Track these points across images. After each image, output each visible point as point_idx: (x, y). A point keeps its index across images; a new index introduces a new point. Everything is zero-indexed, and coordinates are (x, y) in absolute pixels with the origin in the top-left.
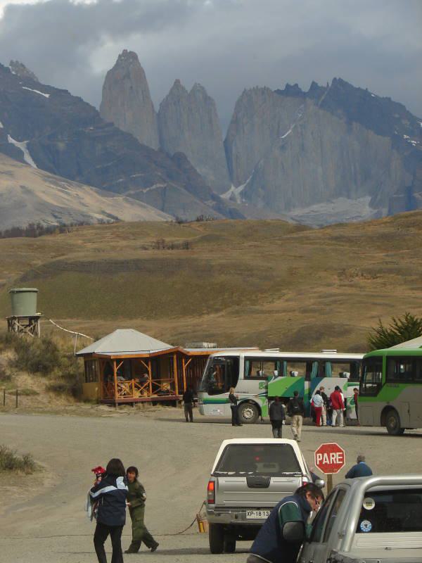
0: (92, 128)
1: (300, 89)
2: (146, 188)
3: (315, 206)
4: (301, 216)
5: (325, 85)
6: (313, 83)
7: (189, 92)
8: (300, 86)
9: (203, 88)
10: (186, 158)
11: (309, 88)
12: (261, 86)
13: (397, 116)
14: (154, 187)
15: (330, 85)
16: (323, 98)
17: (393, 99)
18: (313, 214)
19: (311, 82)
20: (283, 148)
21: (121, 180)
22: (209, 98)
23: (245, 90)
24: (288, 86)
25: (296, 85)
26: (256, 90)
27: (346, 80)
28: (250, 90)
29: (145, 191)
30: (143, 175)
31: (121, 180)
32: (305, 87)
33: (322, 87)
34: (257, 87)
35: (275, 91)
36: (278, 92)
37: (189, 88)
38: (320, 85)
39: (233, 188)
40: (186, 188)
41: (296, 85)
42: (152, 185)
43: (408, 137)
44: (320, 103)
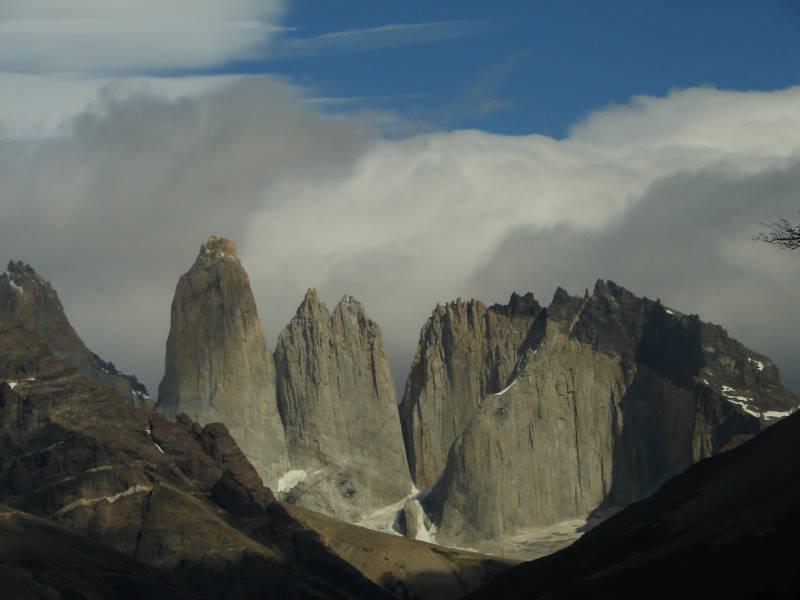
0: (33, 379)
1: (536, 302)
2: (114, 494)
6: (559, 290)
7: (331, 311)
8: (536, 298)
9: (358, 303)
10: (226, 434)
11: (551, 298)
12: (466, 299)
13: (711, 349)
14: (130, 491)
16: (577, 318)
17: (705, 319)
18: (555, 539)
19: (554, 292)
20: (501, 413)
21: (68, 479)
22: (370, 324)
23: (437, 310)
24: (514, 297)
25: (530, 295)
26: (454, 306)
27: (619, 283)
28: (447, 307)
29: (111, 500)
30: (110, 468)
31: (68, 479)
32: (545, 300)
33: (575, 299)
34: (458, 300)
35: (491, 307)
36: (496, 308)
37: (331, 307)
38: (571, 293)
39: (415, 491)
40: (9, 506)
41: (530, 295)
42: (127, 489)
43: (731, 389)
44: (571, 329)
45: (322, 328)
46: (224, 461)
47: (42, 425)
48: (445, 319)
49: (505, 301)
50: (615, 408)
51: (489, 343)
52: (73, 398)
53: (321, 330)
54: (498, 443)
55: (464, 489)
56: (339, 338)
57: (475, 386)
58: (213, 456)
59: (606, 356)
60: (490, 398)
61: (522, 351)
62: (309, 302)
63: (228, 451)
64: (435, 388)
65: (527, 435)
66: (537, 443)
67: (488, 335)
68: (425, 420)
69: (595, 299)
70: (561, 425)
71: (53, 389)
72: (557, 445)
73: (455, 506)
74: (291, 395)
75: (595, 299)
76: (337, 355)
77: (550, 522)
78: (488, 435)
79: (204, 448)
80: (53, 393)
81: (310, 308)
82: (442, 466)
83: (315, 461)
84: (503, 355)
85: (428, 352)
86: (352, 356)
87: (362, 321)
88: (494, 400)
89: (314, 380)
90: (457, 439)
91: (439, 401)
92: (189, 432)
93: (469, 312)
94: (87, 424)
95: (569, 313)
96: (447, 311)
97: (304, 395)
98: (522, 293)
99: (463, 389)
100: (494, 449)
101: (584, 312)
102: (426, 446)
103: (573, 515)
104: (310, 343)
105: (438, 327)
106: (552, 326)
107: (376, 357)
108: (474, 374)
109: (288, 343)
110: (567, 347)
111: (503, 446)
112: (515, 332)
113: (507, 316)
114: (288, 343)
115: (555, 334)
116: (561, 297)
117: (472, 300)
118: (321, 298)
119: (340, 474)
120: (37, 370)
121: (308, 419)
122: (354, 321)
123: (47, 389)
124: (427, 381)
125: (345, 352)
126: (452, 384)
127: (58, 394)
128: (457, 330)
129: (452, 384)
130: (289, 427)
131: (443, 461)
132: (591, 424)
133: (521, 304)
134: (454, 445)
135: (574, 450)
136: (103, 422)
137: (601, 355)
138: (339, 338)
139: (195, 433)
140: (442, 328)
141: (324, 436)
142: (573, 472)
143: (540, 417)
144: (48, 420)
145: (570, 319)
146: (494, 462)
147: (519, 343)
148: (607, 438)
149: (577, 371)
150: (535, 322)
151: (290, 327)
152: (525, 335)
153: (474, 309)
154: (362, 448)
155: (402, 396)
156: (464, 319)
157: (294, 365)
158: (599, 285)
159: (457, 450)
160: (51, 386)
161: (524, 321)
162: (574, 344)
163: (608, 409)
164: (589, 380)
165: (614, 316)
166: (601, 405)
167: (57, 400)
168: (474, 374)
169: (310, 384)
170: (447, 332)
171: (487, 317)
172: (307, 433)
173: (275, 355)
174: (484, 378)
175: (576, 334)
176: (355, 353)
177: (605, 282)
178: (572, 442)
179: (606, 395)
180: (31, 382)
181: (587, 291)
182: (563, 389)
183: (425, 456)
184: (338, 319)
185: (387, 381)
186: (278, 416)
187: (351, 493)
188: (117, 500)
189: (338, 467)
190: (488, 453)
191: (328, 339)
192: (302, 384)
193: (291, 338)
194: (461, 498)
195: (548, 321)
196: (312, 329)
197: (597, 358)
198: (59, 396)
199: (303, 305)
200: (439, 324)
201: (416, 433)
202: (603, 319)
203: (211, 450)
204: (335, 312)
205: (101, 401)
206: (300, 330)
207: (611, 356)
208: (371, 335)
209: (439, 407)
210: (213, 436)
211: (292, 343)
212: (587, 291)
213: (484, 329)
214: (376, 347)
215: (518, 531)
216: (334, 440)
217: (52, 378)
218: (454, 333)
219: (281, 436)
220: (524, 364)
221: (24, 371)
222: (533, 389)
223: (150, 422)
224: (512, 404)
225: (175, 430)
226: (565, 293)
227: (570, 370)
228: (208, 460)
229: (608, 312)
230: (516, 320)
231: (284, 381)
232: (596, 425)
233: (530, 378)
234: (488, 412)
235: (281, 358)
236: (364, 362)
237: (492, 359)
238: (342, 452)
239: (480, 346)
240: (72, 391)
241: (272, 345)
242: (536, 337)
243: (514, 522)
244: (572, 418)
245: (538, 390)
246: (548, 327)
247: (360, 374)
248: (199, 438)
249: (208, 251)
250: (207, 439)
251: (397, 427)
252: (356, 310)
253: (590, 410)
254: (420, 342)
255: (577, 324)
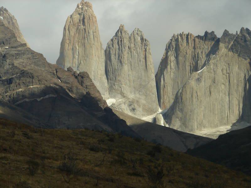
0: (8, 47)
3: (222, 127)
4: (209, 135)
5: (235, 33)
6: (226, 30)
7: (130, 34)
8: (215, 34)
10: (88, 77)
12: (186, 32)
14: (47, 96)
15: (239, 33)
16: (232, 43)
20: (199, 80)
21: (20, 90)
22: (146, 40)
25: (213, 32)
26: (181, 35)
29: (39, 100)
31: (20, 90)
33: (232, 34)
34: (183, 33)
35: (196, 37)
36: (199, 37)
37: (130, 32)
38: (230, 32)
39: (160, 111)
41: (213, 32)
44: (230, 47)
45: (126, 41)
46: (86, 88)
47: (10, 66)
48: (177, 40)
49: (202, 34)
50: (246, 82)
51: (195, 51)
52: (24, 57)
53: (125, 42)
54: (197, 92)
55: (182, 110)
56: (132, 45)
57: (188, 68)
58: (82, 85)
59: (243, 59)
60: (194, 73)
61: (208, 55)
62: (121, 30)
63: (88, 84)
64: (171, 69)
65: (208, 90)
66: (212, 93)
67: (194, 48)
68: (166, 81)
69: (240, 35)
70: (223, 86)
71: (16, 52)
72: (221, 95)
73: (177, 118)
74: (111, 67)
75: (240, 35)
76: (131, 52)
77: (216, 126)
78: (192, 88)
79: (78, 82)
80: (16, 54)
81: (121, 33)
82: (172, 101)
83: (120, 96)
84: (200, 56)
85: (169, 53)
86: (137, 53)
87: (142, 39)
88: (196, 74)
89: (121, 62)
90: (179, 90)
91: (172, 74)
92: (72, 75)
93: (187, 38)
94: (29, 68)
95: (229, 41)
96: (178, 37)
97: (117, 68)
98: (210, 31)
99: (183, 69)
100: (195, 95)
101: (235, 40)
102: (166, 92)
103: (225, 124)
104: (120, 47)
105: (174, 43)
106: (222, 45)
107: (147, 54)
108: (188, 64)
109: (111, 46)
110: (228, 55)
111: (198, 94)
112: (206, 47)
113: (203, 40)
114: (111, 46)
115: (223, 49)
116: (226, 33)
117: (189, 33)
118: (125, 28)
119: (130, 102)
120: (9, 44)
121: (118, 78)
122: (139, 38)
123: (13, 52)
124: (168, 65)
125: (134, 51)
126: (178, 67)
127: (17, 54)
128: (182, 45)
129: (178, 67)
130: (109, 81)
131: (173, 99)
132: (235, 87)
133: (209, 36)
134: (178, 92)
135: (228, 97)
136: (36, 67)
137: (242, 59)
138: (132, 45)
139: (75, 76)
140: (174, 45)
141: (124, 86)
142: (227, 107)
143: (214, 83)
144: (13, 64)
145: (229, 43)
146: (194, 100)
147: (207, 52)
148: (242, 93)
149: (231, 65)
150: (214, 43)
151: (112, 40)
152: (210, 49)
153: (189, 37)
154: (139, 92)
155: (157, 71)
156: (185, 41)
157: (113, 55)
158: (242, 29)
159: (179, 94)
160: (15, 51)
161: (210, 43)
162: (230, 53)
163: (243, 81)
164: (236, 69)
165: (248, 43)
166: (240, 79)
167: (17, 57)
168: (188, 64)
169: (119, 64)
170: (177, 45)
171: (194, 40)
172: (117, 84)
173: (106, 51)
174: (192, 65)
175: (232, 49)
176: (139, 52)
177: (245, 29)
178: (227, 94)
179: (242, 75)
180: (7, 49)
181: (237, 31)
182: (225, 72)
183: (165, 96)
184: (132, 38)
185: (151, 64)
186: (105, 76)
187: (134, 109)
188: (41, 100)
189: (129, 98)
190: (192, 96)
191: (128, 46)
192: (116, 64)
193: (113, 44)
194: (179, 114)
195: (220, 43)
196: (121, 41)
197: (240, 60)
198: (18, 55)
199: (118, 31)
200: (174, 42)
201: (162, 87)
202: (243, 44)
203: (82, 83)
204: (131, 35)
205: (35, 59)
206: (116, 41)
207: (246, 59)
208: (146, 45)
209: (172, 76)
210: (82, 77)
211: (113, 46)
212: (237, 31)
213: (193, 45)
214: (147, 50)
215: (203, 129)
216: (128, 87)
217: (15, 47)
218: (180, 46)
219: (106, 85)
220: (209, 61)
221: (4, 43)
222: (212, 71)
223: (56, 70)
224: (203, 77)
225: (67, 73)
226: (228, 32)
227: (228, 64)
228: (80, 87)
229: (245, 41)
230: (206, 42)
231: (108, 62)
232: (238, 87)
233: (211, 66)
234: (193, 79)
235: (108, 52)
236: (142, 56)
237: (195, 58)
238: (131, 92)
239: (191, 52)
240: (24, 54)
241: (105, 47)
242: (214, 50)
243: (201, 125)
244: (228, 84)
245: (214, 72)
246: (220, 46)
247: (140, 61)
248: (76, 77)
249: (80, 6)
250: (80, 78)
251: (154, 84)
252: (140, 34)
253: (235, 81)
254: (166, 49)
255: (232, 45)
